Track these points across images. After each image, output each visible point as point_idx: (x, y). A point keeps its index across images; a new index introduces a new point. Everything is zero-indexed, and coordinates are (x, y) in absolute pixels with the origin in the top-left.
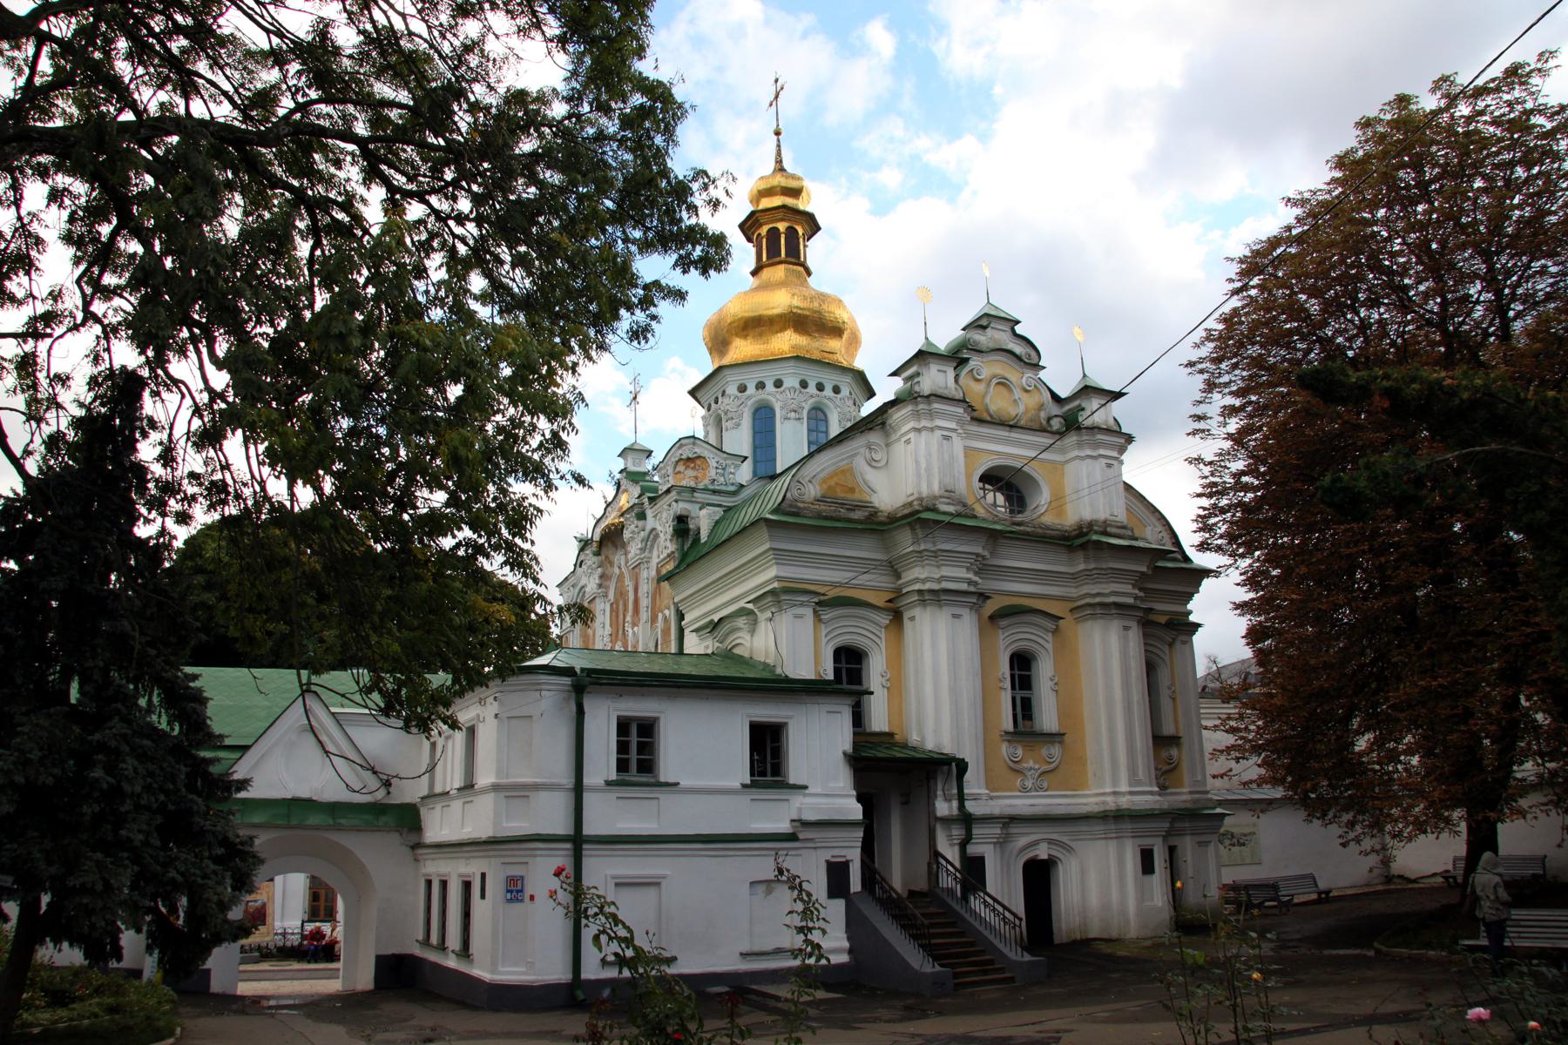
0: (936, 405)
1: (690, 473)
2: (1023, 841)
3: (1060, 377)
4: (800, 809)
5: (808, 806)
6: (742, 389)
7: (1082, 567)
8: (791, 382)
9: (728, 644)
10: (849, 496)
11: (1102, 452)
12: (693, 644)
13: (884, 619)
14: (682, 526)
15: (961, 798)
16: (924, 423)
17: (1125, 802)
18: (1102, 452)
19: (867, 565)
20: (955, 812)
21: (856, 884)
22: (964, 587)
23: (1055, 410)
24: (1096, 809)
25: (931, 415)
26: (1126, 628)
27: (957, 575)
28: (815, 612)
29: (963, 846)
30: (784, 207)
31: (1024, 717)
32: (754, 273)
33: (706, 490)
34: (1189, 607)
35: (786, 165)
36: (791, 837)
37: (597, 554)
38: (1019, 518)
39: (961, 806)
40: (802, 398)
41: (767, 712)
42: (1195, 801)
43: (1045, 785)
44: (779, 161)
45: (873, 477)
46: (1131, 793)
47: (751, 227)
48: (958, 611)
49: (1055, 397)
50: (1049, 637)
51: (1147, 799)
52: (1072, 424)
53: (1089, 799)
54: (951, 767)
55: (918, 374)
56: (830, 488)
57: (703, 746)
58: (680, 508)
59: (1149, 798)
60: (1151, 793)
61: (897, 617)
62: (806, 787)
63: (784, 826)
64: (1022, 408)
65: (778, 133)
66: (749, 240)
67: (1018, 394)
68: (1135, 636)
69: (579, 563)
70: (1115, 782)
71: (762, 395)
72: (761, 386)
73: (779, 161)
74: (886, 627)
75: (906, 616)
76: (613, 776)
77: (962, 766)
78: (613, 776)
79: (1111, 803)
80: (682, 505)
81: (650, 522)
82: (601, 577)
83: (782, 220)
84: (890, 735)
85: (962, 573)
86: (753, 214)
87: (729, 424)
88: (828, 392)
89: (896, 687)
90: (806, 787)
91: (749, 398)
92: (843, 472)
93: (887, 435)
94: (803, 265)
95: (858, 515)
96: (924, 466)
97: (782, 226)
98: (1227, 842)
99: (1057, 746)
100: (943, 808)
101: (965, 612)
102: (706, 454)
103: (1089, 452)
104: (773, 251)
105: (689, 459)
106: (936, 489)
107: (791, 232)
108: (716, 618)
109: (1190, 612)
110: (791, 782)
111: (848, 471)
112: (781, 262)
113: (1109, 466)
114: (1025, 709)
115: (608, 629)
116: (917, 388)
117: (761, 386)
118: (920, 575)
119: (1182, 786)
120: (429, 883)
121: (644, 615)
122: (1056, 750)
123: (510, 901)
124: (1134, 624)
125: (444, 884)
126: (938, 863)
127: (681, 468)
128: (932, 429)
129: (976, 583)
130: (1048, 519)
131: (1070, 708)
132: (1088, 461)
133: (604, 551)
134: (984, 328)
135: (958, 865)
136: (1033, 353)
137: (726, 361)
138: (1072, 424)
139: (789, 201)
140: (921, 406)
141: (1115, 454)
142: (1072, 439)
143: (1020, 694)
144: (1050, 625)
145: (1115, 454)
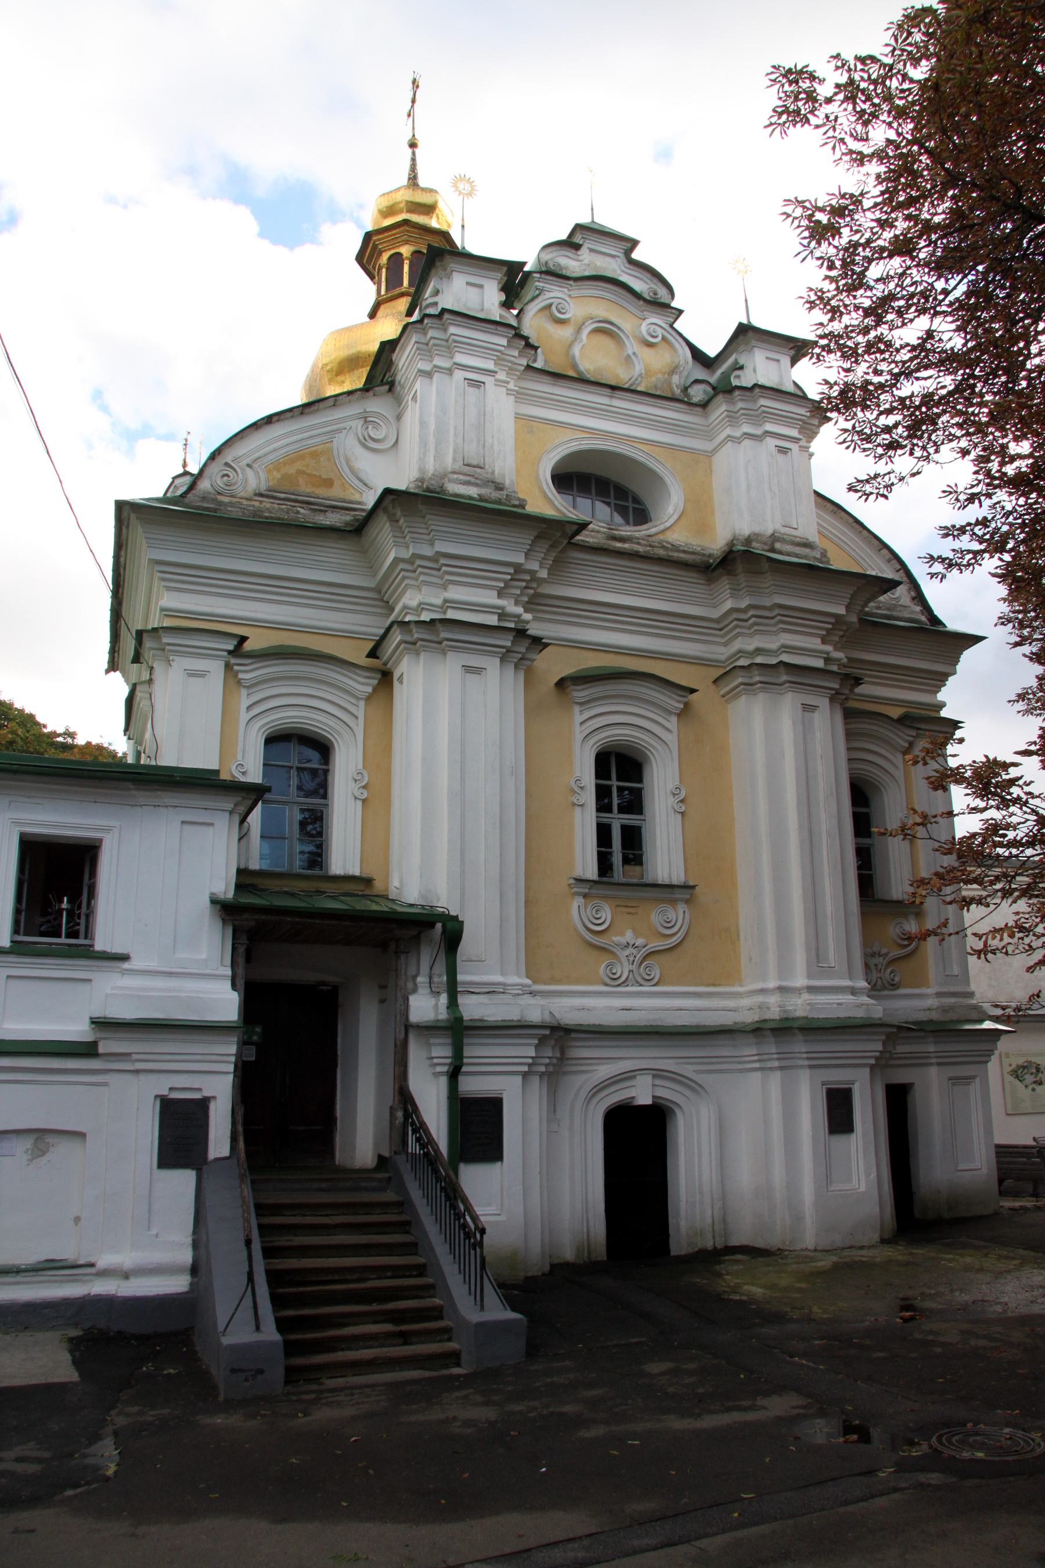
0: (452, 330)
2: (604, 1071)
7: (728, 605)
10: (321, 492)
11: (769, 427)
13: (364, 685)
15: (453, 990)
16: (438, 361)
17: (800, 1006)
20: (443, 1014)
23: (701, 373)
24: (749, 1018)
25: (449, 347)
26: (808, 708)
27: (478, 599)
28: (228, 666)
29: (454, 1074)
30: (406, 222)
34: (941, 696)
36: (87, 1050)
39: (453, 1003)
41: (61, 818)
42: (945, 1010)
43: (656, 973)
46: (810, 989)
47: (369, 261)
48: (474, 661)
49: (697, 355)
50: (673, 723)
51: (846, 998)
53: (741, 1003)
54: (435, 932)
56: (285, 477)
59: (849, 998)
60: (853, 991)
61: (386, 678)
62: (124, 958)
63: (74, 1028)
64: (638, 368)
65: (413, 145)
67: (632, 346)
68: (826, 725)
70: (784, 967)
73: (413, 179)
74: (369, 699)
75: (396, 675)
79: (774, 1008)
83: (407, 242)
85: (490, 598)
89: (376, 799)
90: (124, 958)
92: (315, 455)
96: (432, 427)
97: (406, 251)
98: (1029, 1079)
99: (681, 908)
100: (425, 1006)
101: (492, 665)
103: (747, 429)
106: (449, 462)
109: (942, 705)
110: (99, 946)
111: (322, 453)
114: (622, 846)
118: (417, 599)
119: (925, 984)
122: (678, 914)
124: (823, 703)
128: (450, 371)
130: (679, 537)
131: (709, 841)
132: (747, 443)
136: (662, 292)
140: (431, 333)
142: (720, 408)
143: (617, 821)
145: (794, 433)
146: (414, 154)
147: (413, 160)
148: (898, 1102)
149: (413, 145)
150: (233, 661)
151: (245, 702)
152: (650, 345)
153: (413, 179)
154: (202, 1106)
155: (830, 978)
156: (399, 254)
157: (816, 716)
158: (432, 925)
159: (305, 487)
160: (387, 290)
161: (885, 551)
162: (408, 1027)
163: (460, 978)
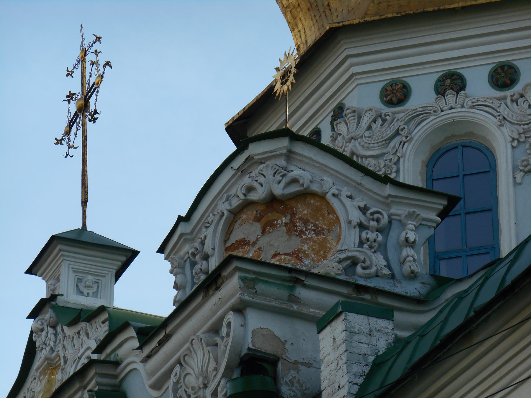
6: (396, 94)
58: (256, 329)
71: (455, 109)
72: (451, 83)
80: (255, 320)
102: (327, 184)
105: (272, 201)
117: (451, 83)
127: (247, 229)
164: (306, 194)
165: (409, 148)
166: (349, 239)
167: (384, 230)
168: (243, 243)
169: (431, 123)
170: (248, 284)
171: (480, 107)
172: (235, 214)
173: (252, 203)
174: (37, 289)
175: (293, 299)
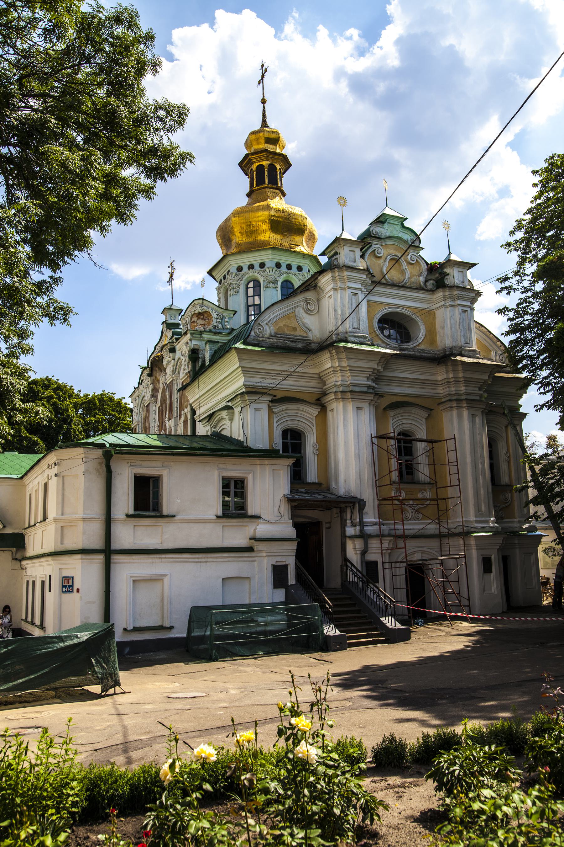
1: (200, 322)
3: (432, 253)
4: (255, 531)
5: (262, 529)
8: (270, 264)
9: (218, 429)
10: (293, 333)
11: (459, 302)
12: (202, 430)
14: (194, 354)
15: (362, 524)
18: (459, 302)
19: (304, 376)
21: (292, 581)
22: (365, 389)
26: (474, 416)
28: (269, 407)
29: (364, 553)
31: (408, 473)
32: (248, 195)
33: (210, 331)
34: (520, 402)
35: (268, 123)
36: (250, 549)
37: (150, 375)
38: (405, 346)
39: (362, 530)
40: (277, 274)
44: (264, 121)
45: (310, 321)
48: (360, 404)
52: (441, 284)
55: (336, 253)
57: (193, 492)
61: (323, 408)
62: (259, 517)
66: (246, 174)
69: (141, 382)
73: (264, 121)
75: (329, 409)
76: (131, 512)
77: (361, 504)
78: (131, 512)
80: (194, 342)
81: (178, 354)
82: (153, 390)
84: (319, 484)
86: (247, 155)
87: (231, 292)
88: (294, 269)
91: (244, 275)
93: (319, 294)
94: (279, 189)
95: (300, 345)
96: (339, 312)
97: (265, 163)
98: (551, 554)
100: (350, 531)
101: (366, 405)
104: (260, 181)
105: (199, 313)
107: (272, 168)
108: (211, 412)
112: (265, 188)
113: (464, 311)
115: (157, 423)
116: (336, 263)
119: (514, 518)
120: (28, 582)
121: (175, 414)
123: (65, 592)
125: (34, 582)
126: (347, 566)
127: (195, 319)
128: (344, 289)
129: (374, 388)
133: (154, 373)
134: (383, 223)
135: (360, 568)
137: (229, 253)
138: (441, 284)
139: (270, 147)
141: (468, 304)
142: (440, 294)
143: (405, 458)
144: (424, 414)
145: (468, 304)
146: (264, 107)
147: (264, 110)
148: (505, 561)
149: (263, 102)
150: (271, 405)
151: (275, 420)
152: (412, 264)
153: (264, 123)
154: (286, 566)
155: (483, 517)
156: (262, 166)
157: (477, 418)
158: (354, 503)
159: (287, 331)
160: (257, 185)
161: (499, 343)
162: (346, 537)
163: (364, 520)
164: (206, 312)
165: (242, 282)
166: (214, 321)
167: (222, 319)
168: (194, 322)
169: (247, 276)
170: (192, 334)
171: (256, 274)
172: (192, 315)
173: (195, 314)
174: (163, 318)
175: (201, 337)
